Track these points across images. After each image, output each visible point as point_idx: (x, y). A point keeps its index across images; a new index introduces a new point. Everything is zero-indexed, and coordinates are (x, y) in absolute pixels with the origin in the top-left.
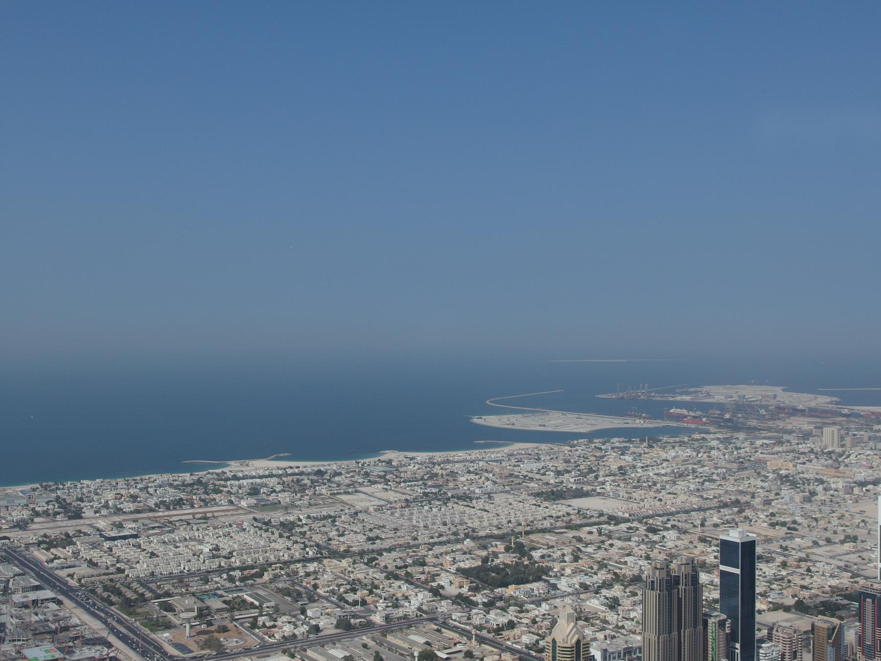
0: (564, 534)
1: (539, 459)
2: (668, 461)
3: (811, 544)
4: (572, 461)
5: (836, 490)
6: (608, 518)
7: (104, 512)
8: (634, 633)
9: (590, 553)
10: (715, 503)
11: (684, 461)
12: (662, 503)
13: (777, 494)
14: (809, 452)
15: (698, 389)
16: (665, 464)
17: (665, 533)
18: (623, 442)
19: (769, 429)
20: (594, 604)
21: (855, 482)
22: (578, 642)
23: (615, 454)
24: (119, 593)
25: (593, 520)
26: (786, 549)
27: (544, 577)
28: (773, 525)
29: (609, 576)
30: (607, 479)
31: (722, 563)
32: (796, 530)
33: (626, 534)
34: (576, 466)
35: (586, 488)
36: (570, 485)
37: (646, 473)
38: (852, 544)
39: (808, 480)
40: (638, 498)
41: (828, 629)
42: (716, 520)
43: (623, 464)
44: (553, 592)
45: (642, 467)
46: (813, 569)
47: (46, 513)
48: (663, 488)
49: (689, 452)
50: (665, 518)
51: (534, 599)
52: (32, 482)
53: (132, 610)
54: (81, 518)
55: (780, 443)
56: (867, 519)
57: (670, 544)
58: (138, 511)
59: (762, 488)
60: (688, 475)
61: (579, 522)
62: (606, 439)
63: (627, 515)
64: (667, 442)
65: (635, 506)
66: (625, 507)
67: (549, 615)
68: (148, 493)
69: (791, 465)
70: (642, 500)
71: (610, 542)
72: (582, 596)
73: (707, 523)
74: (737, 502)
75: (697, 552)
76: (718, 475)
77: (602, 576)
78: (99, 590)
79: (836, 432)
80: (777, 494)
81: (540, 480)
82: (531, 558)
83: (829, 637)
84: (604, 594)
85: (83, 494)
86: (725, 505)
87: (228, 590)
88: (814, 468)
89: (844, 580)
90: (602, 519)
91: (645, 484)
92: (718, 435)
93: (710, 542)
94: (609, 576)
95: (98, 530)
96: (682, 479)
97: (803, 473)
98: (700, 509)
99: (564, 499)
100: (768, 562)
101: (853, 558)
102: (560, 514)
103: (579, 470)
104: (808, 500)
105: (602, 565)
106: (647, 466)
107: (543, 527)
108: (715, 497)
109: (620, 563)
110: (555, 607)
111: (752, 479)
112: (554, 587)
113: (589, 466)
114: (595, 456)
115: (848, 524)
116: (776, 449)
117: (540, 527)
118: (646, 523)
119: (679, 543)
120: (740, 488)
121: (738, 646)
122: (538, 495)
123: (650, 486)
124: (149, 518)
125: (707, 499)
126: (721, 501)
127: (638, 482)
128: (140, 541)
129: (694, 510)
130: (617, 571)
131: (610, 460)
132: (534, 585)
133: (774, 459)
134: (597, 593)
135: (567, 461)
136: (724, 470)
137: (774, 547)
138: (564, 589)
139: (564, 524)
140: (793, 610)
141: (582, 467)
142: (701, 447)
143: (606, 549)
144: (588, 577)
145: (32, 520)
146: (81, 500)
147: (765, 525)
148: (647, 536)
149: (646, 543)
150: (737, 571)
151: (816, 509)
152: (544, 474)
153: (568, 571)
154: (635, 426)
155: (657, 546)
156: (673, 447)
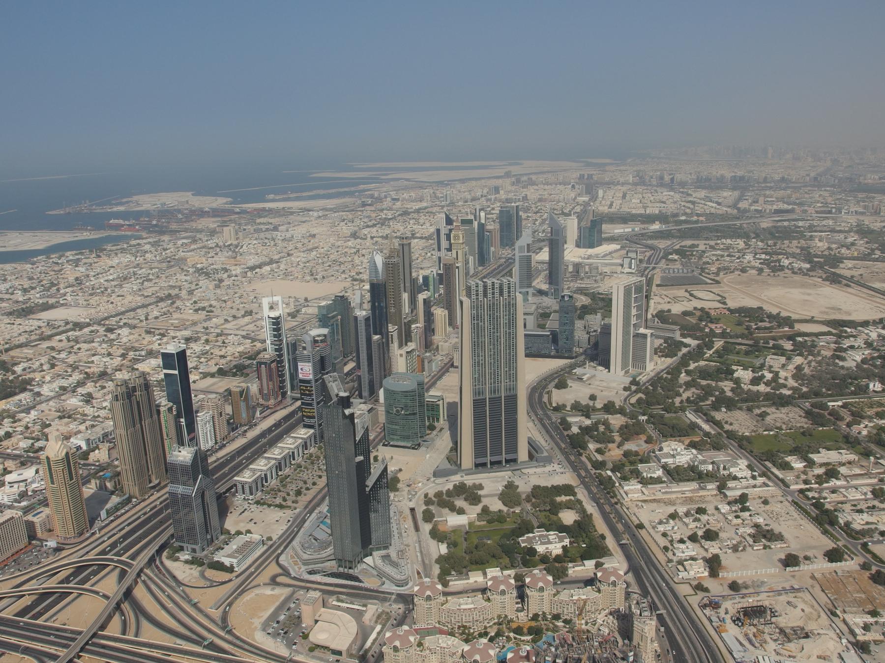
0: (39, 346)
1: (5, 280)
2: (113, 267)
3: (223, 322)
4: (35, 277)
5: (236, 276)
6: (73, 325)
8: (108, 419)
9: (64, 359)
10: (153, 300)
11: (126, 266)
12: (114, 305)
13: (197, 285)
14: (216, 246)
15: (130, 199)
16: (112, 270)
17: (120, 332)
18: (76, 254)
19: (186, 230)
20: (73, 402)
22: (67, 453)
23: (70, 267)
25: (61, 329)
26: (207, 328)
27: (28, 387)
28: (196, 311)
29: (82, 376)
30: (67, 290)
31: (166, 366)
32: (212, 312)
33: (89, 337)
34: (39, 282)
35: (52, 301)
36: (37, 301)
37: (98, 281)
38: (249, 317)
39: (217, 270)
40: (95, 304)
41: (240, 392)
42: (156, 313)
43: (78, 275)
44: (38, 399)
45: (94, 276)
46: (226, 341)
48: (113, 292)
49: (128, 258)
50: (118, 318)
51: (23, 408)
55: (195, 241)
56: (257, 295)
57: (125, 340)
59: (186, 281)
60: (131, 278)
61: (49, 333)
62: (61, 253)
63: (88, 320)
64: (110, 251)
65: (93, 311)
66: (85, 313)
67: (38, 419)
69: (204, 259)
70: (98, 305)
71: (78, 346)
72: (63, 397)
73: (149, 317)
74: (170, 295)
75: (145, 342)
76: (153, 274)
77: (76, 377)
79: (232, 230)
80: (197, 285)
81: (10, 299)
82: (14, 372)
83: (241, 397)
84: (80, 392)
86: (161, 300)
88: (221, 259)
89: (247, 346)
90: (68, 327)
91: (98, 291)
92: (149, 240)
93: (154, 332)
94: (82, 376)
96: (126, 282)
97: (213, 264)
98: (144, 306)
99: (34, 313)
100: (196, 341)
101: (251, 327)
102: (33, 328)
103: (42, 286)
104: (217, 287)
105: (74, 367)
106: (98, 274)
107: (20, 342)
108: (153, 294)
109: (89, 363)
110: (42, 411)
111: (178, 275)
112: (39, 394)
113: (50, 280)
114: (54, 271)
115: (245, 301)
116: (193, 247)
117: (17, 343)
118: (104, 325)
119: (131, 337)
120: (170, 284)
121: (182, 420)
122: (10, 314)
123: (102, 292)
125: (147, 296)
126: (158, 296)
127: (93, 289)
129: (139, 307)
130: (87, 370)
131: (68, 272)
132: (22, 396)
133: (192, 256)
134: (74, 392)
135: (31, 279)
136: (157, 270)
137: (199, 328)
138: (47, 394)
139: (38, 337)
140: (216, 375)
141: (44, 282)
142: (138, 252)
143: (75, 353)
144: (64, 380)
147: (191, 311)
148: (106, 336)
149: (106, 342)
150: (176, 372)
151: (224, 293)
152: (12, 294)
153: (48, 378)
154: (83, 238)
155: (115, 343)
156: (116, 254)
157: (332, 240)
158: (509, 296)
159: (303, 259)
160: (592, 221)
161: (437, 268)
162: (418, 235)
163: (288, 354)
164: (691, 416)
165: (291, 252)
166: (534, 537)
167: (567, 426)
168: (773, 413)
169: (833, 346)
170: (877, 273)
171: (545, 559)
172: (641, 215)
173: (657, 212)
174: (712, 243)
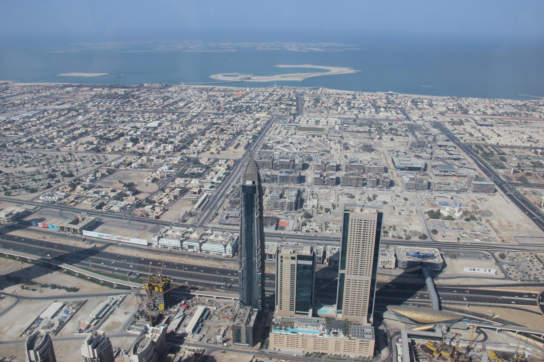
7: (478, 113)
24: (482, 149)
47: (453, 110)
52: (448, 96)
53: (486, 157)
54: (467, 114)
58: (493, 115)
68: (499, 107)
78: (473, 147)
85: (469, 104)
87: (533, 157)
95: (475, 120)
124: (499, 119)
128: (494, 128)
145: (447, 112)
146: (468, 106)
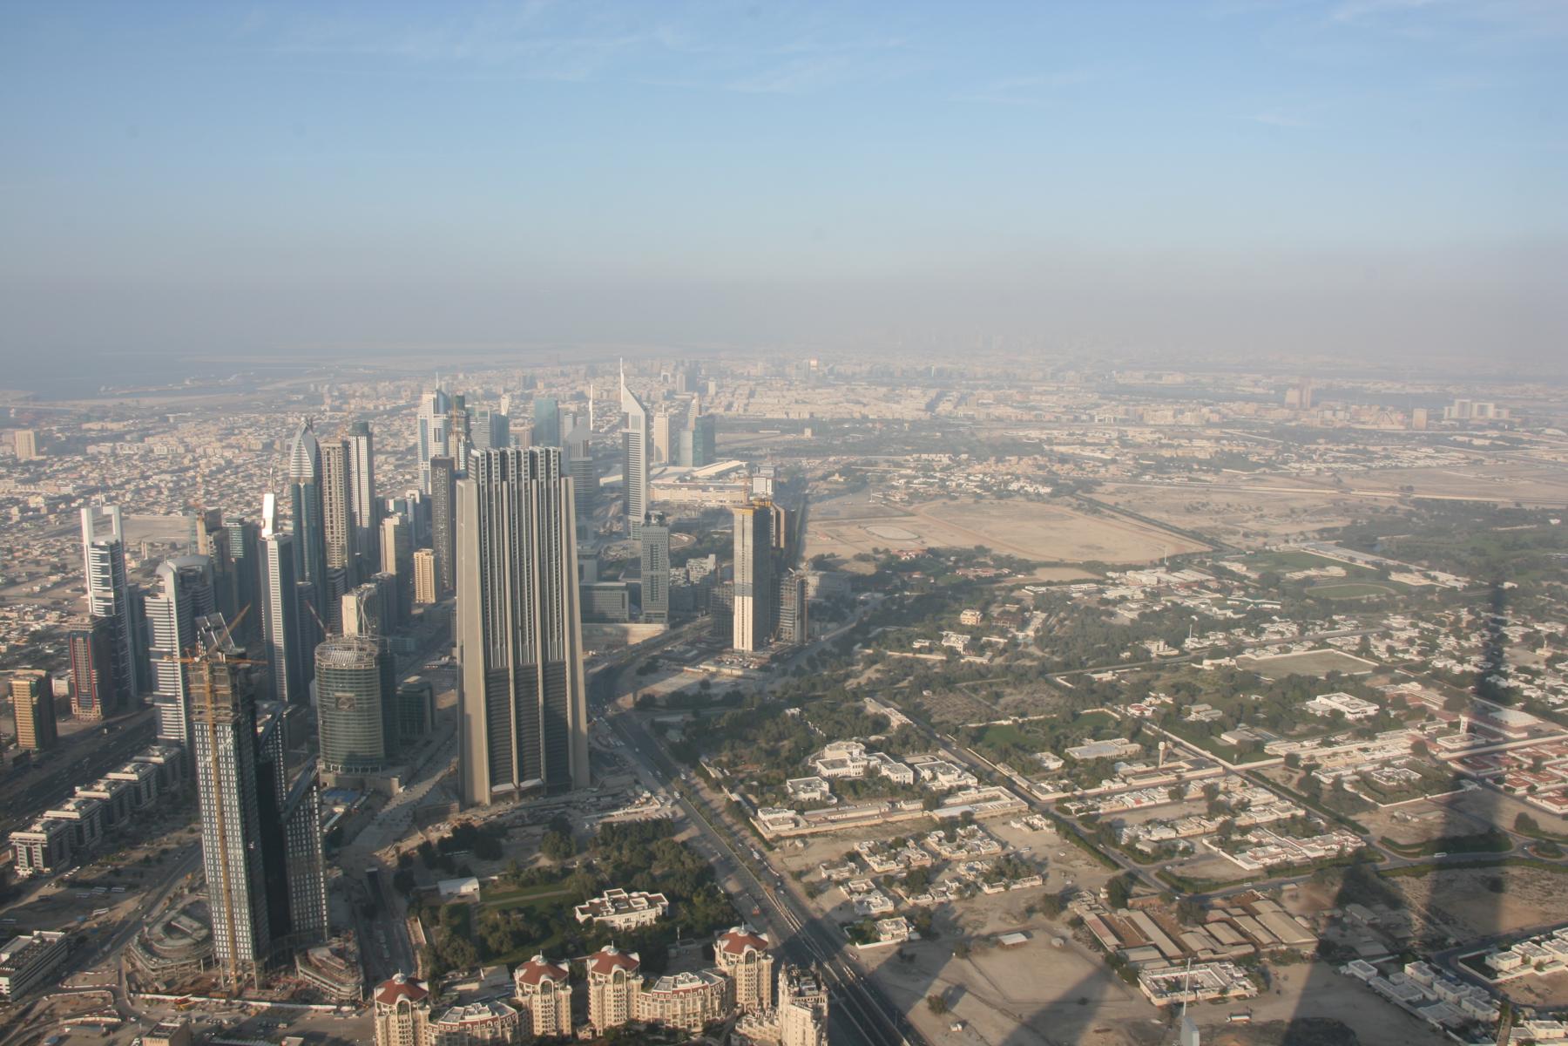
5: (37, 510)
21: (60, 497)
157: (228, 454)
158: (548, 477)
159: (171, 485)
160: (697, 419)
161: (422, 487)
162: (389, 448)
163: (133, 622)
164: (872, 707)
165: (149, 473)
166: (603, 903)
167: (662, 729)
168: (1011, 694)
169: (1097, 597)
170: (1152, 498)
171: (627, 940)
172: (780, 421)
173: (807, 416)
174: (897, 458)
